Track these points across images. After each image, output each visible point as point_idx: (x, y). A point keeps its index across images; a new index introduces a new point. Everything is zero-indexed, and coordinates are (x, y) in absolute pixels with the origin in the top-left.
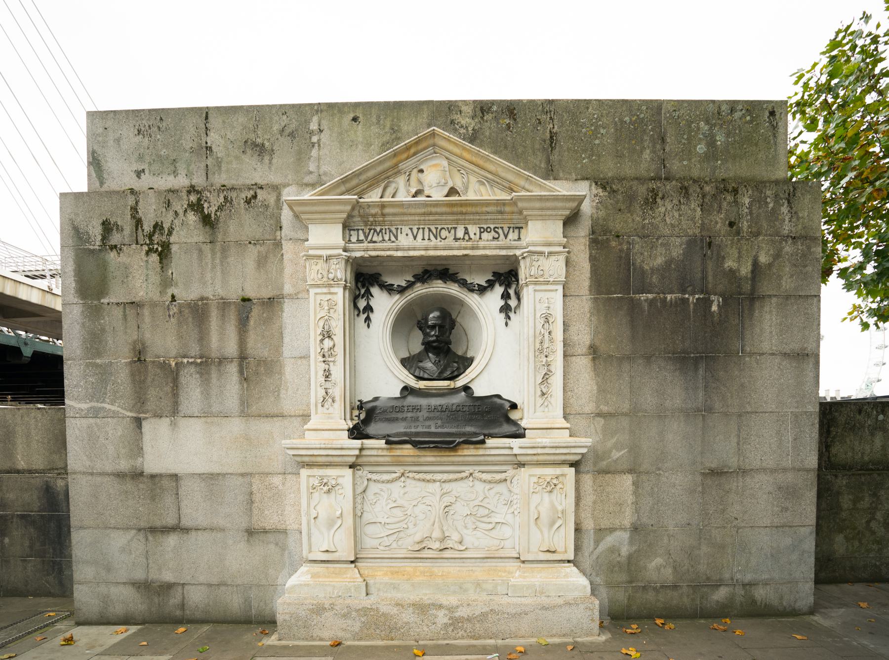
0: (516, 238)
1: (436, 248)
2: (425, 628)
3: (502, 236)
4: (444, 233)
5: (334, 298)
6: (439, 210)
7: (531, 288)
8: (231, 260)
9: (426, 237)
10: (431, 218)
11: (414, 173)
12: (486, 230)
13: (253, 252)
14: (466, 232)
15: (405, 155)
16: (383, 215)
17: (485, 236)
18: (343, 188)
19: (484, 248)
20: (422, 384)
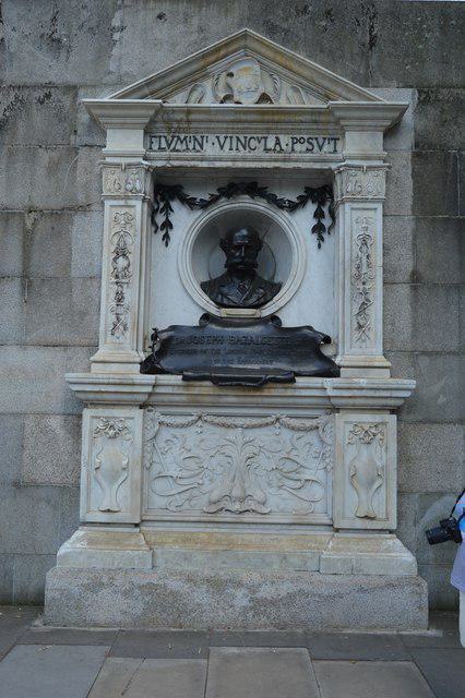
1: (244, 160)
2: (221, 614)
3: (316, 148)
4: (253, 143)
6: (250, 117)
7: (348, 206)
8: (18, 165)
11: (223, 79)
12: (299, 141)
13: (45, 157)
14: (278, 142)
15: (213, 58)
16: (189, 121)
17: (298, 147)
18: (146, 91)
19: (296, 161)
20: (224, 312)
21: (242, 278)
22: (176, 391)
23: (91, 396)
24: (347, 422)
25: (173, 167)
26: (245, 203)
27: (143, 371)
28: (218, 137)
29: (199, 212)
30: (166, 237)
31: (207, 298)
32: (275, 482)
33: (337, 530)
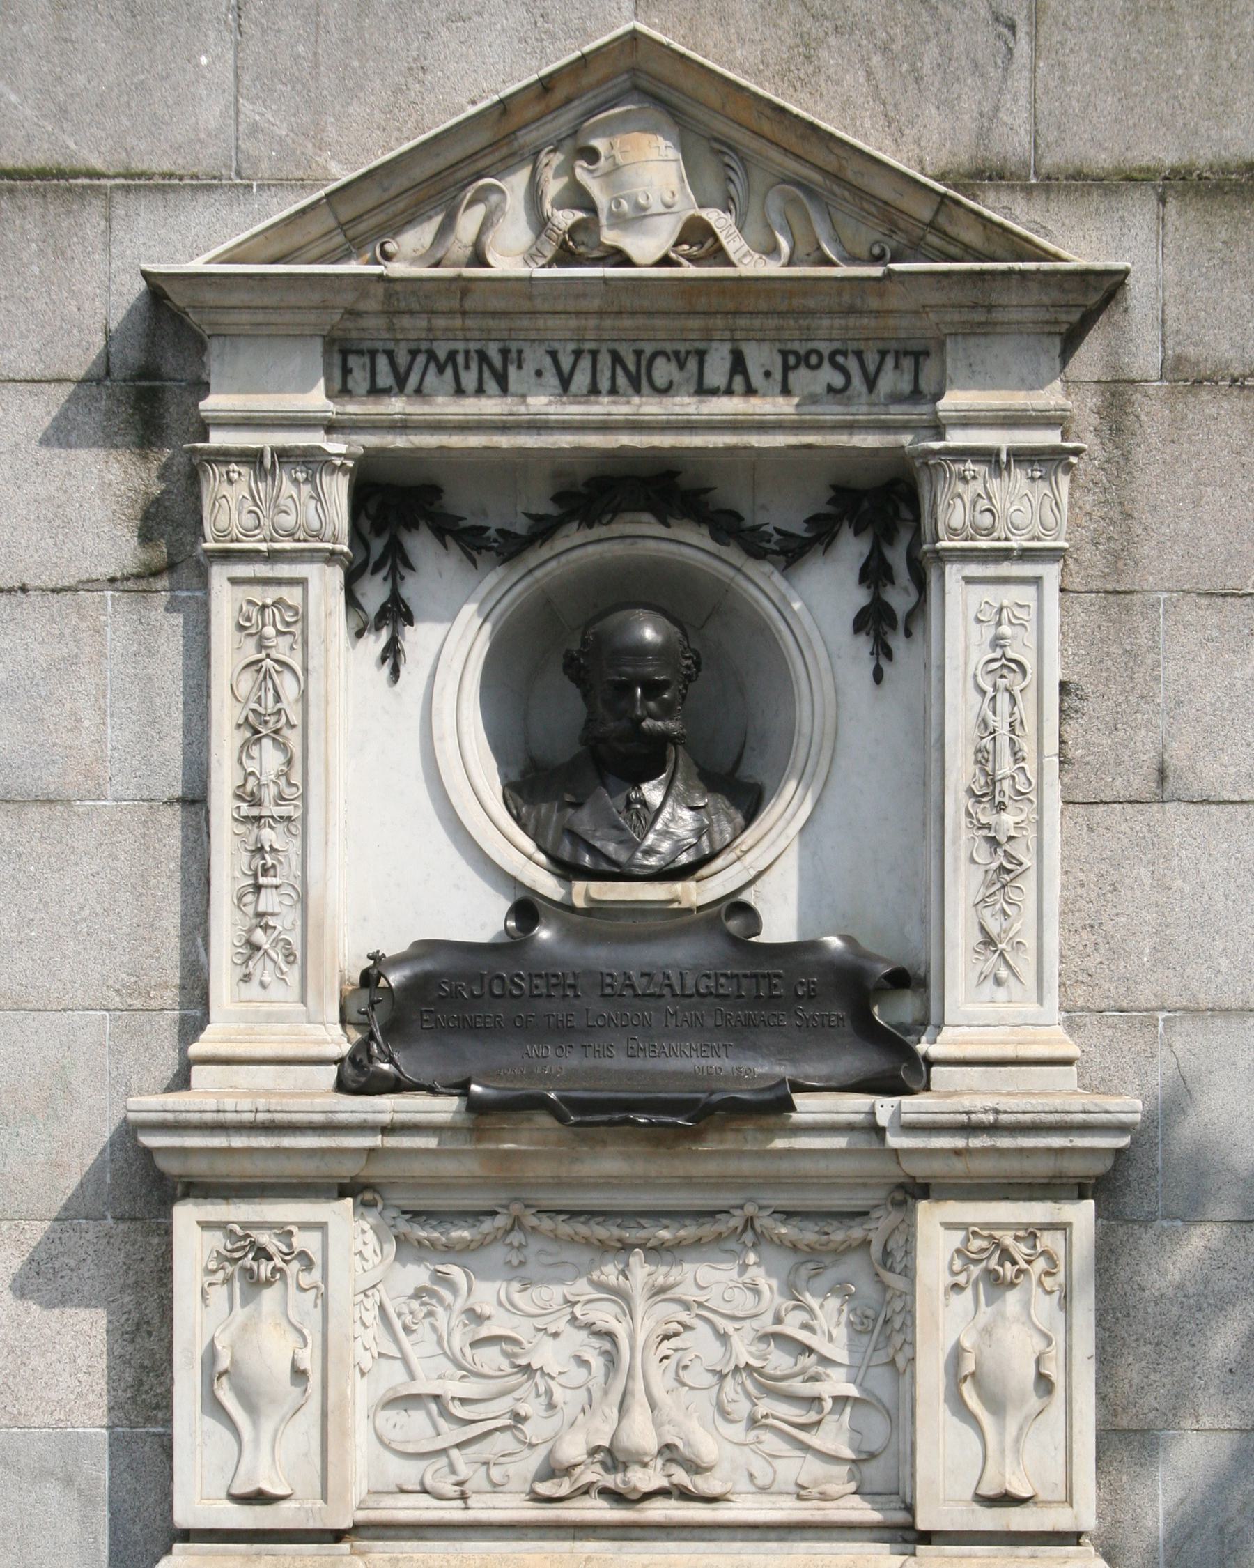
0: (906, 386)
3: (858, 382)
5: (292, 595)
9: (604, 384)
12: (804, 360)
24: (949, 1226)
27: (341, 1086)
29: (500, 571)
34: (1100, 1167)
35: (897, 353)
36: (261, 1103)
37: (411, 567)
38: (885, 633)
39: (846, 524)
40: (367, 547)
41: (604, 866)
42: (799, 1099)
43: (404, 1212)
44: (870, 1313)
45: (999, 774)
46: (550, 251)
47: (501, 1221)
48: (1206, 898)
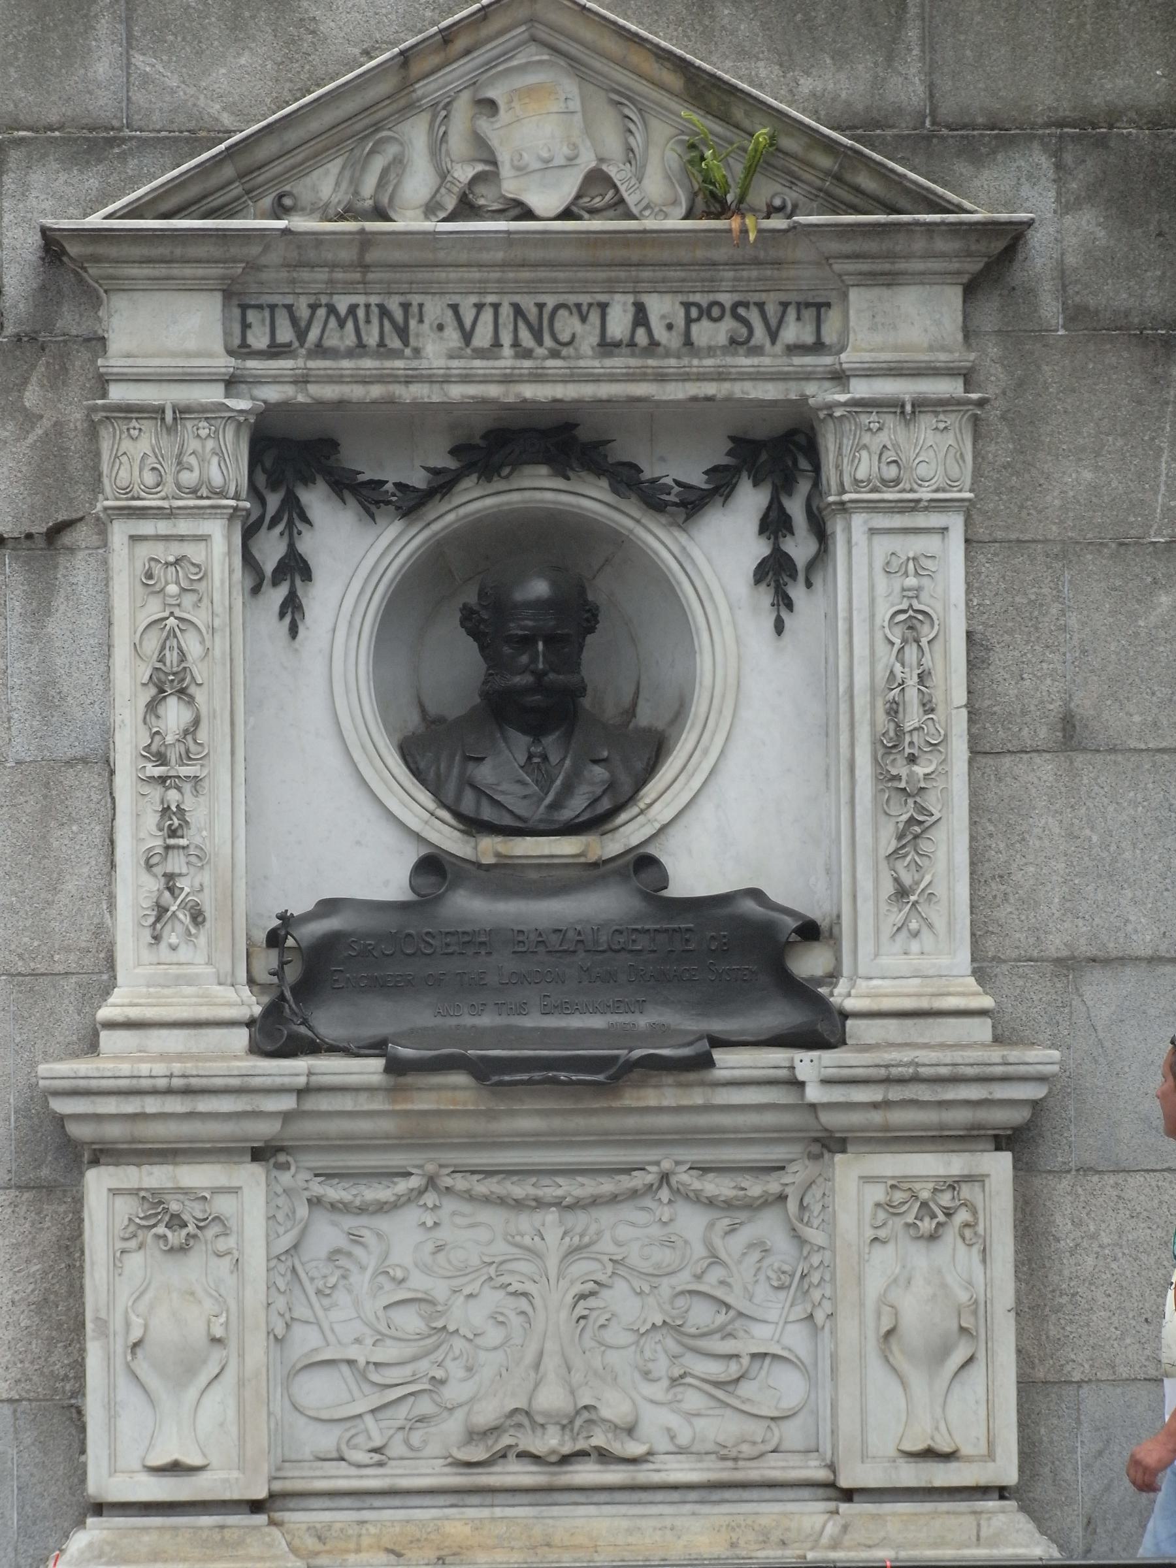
3: (760, 334)
4: (567, 325)
5: (195, 552)
9: (506, 339)
10: (526, 274)
12: (706, 312)
14: (641, 317)
16: (365, 267)
17: (706, 333)
21: (536, 731)
22: (365, 1103)
23: (114, 1131)
24: (867, 1179)
25: (320, 403)
26: (538, 490)
27: (256, 1049)
28: (455, 308)
30: (292, 607)
31: (425, 798)
32: (661, 1367)
33: (848, 1495)
34: (1019, 1116)
35: (798, 304)
36: (177, 1067)
37: (306, 520)
38: (786, 584)
39: (745, 474)
40: (263, 502)
41: (508, 821)
42: (718, 1055)
43: (316, 1175)
44: (786, 1268)
45: (908, 725)
46: (450, 203)
47: (415, 1182)
48: (1113, 848)
